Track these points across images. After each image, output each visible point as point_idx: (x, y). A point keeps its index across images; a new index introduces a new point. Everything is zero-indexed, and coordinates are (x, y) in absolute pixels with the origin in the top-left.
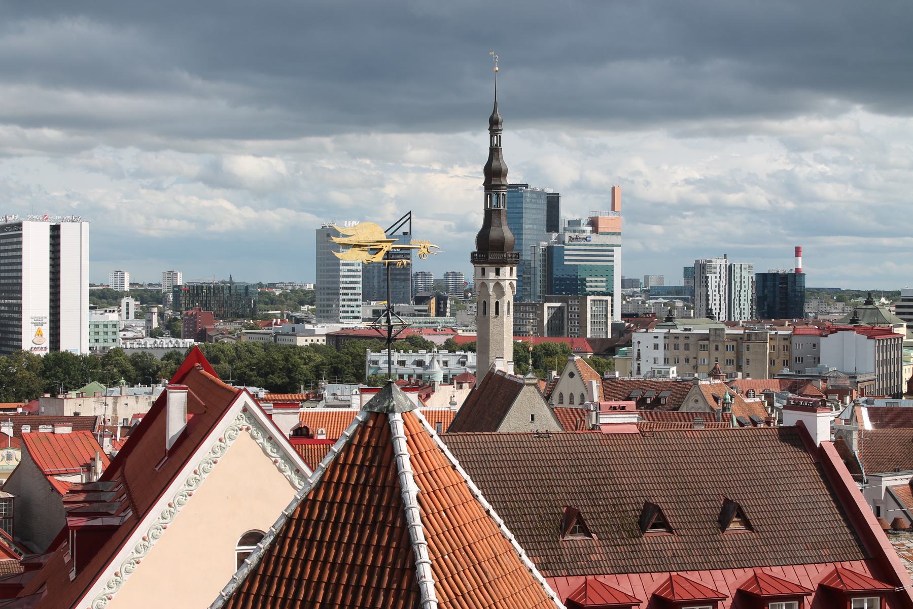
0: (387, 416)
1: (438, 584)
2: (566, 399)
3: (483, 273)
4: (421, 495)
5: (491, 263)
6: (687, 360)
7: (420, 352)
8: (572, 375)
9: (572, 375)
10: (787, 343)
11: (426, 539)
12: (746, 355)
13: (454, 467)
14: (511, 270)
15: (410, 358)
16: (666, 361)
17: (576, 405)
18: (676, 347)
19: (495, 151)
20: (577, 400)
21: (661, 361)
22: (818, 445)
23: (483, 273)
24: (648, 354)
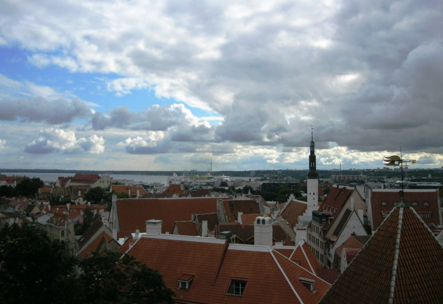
0: (400, 208)
1: (401, 255)
4: (403, 230)
13: (422, 224)
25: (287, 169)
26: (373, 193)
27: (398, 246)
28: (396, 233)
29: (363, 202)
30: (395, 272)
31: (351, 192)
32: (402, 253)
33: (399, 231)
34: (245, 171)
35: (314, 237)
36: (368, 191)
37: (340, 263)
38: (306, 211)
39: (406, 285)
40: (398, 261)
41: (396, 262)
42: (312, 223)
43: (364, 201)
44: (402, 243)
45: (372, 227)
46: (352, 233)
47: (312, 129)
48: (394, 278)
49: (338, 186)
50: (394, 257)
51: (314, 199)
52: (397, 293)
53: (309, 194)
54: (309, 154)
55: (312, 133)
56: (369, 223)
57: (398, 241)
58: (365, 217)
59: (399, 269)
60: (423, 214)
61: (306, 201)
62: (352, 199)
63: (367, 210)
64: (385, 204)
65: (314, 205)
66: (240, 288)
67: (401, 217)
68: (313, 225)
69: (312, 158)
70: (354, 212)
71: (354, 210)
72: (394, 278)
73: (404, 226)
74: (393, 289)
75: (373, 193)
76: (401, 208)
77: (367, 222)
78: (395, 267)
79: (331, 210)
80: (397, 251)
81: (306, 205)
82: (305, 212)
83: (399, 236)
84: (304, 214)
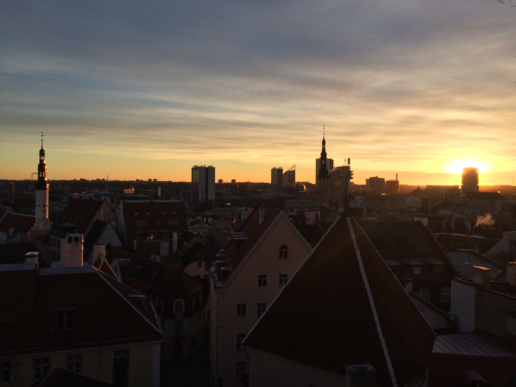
3: (320, 181)
7: (300, 200)
8: (341, 207)
9: (341, 207)
14: (328, 180)
22: (424, 226)
23: (320, 181)
25: (457, 182)
34: (234, 181)
35: (55, 252)
38: (35, 224)
42: (51, 237)
43: (114, 211)
47: (42, 136)
51: (44, 211)
53: (38, 206)
54: (38, 163)
55: (42, 140)
58: (116, 227)
60: (172, 222)
61: (35, 215)
62: (102, 211)
65: (44, 218)
66: (65, 318)
68: (52, 239)
69: (41, 167)
70: (109, 223)
75: (125, 205)
79: (69, 221)
81: (35, 218)
82: (33, 226)
84: (32, 228)
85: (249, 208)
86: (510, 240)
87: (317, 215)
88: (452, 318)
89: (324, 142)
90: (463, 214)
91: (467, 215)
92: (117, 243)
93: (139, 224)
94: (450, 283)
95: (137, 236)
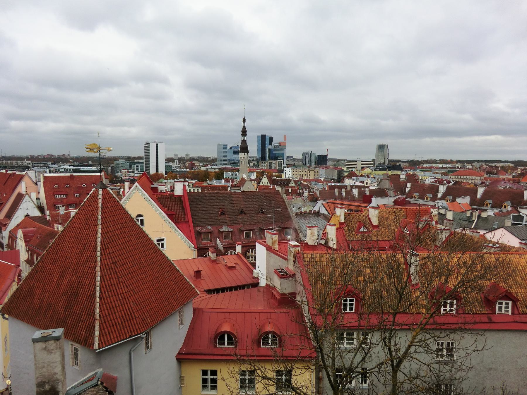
1: (103, 229)
2: (264, 183)
5: (243, 152)
6: (296, 175)
8: (265, 178)
9: (265, 178)
10: (318, 171)
11: (102, 219)
12: (309, 173)
15: (234, 173)
16: (291, 174)
17: (266, 185)
18: (294, 171)
19: (244, 127)
20: (266, 183)
21: (290, 175)
24: (288, 173)
26: (45, 178)
27: (100, 222)
28: (97, 211)
29: (35, 186)
30: (99, 244)
31: (21, 178)
32: (103, 227)
33: (100, 209)
36: (40, 175)
37: (16, 243)
39: (110, 253)
40: (101, 234)
41: (99, 235)
43: (36, 184)
44: (103, 219)
45: (46, 208)
46: (26, 214)
48: (99, 249)
49: (6, 171)
50: (97, 231)
52: (103, 261)
56: (42, 205)
57: (100, 217)
58: (38, 199)
59: (102, 241)
63: (39, 193)
64: (57, 186)
67: (100, 197)
70: (27, 196)
71: (27, 194)
72: (99, 249)
73: (103, 204)
74: (99, 259)
75: (45, 178)
76: (100, 189)
77: (40, 203)
78: (99, 239)
80: (100, 227)
83: (100, 213)
85: (187, 179)
86: (377, 205)
87: (184, 185)
88: (255, 276)
89: (244, 121)
90: (363, 183)
91: (367, 184)
92: (37, 213)
93: (58, 196)
94: (255, 246)
95: (57, 207)
